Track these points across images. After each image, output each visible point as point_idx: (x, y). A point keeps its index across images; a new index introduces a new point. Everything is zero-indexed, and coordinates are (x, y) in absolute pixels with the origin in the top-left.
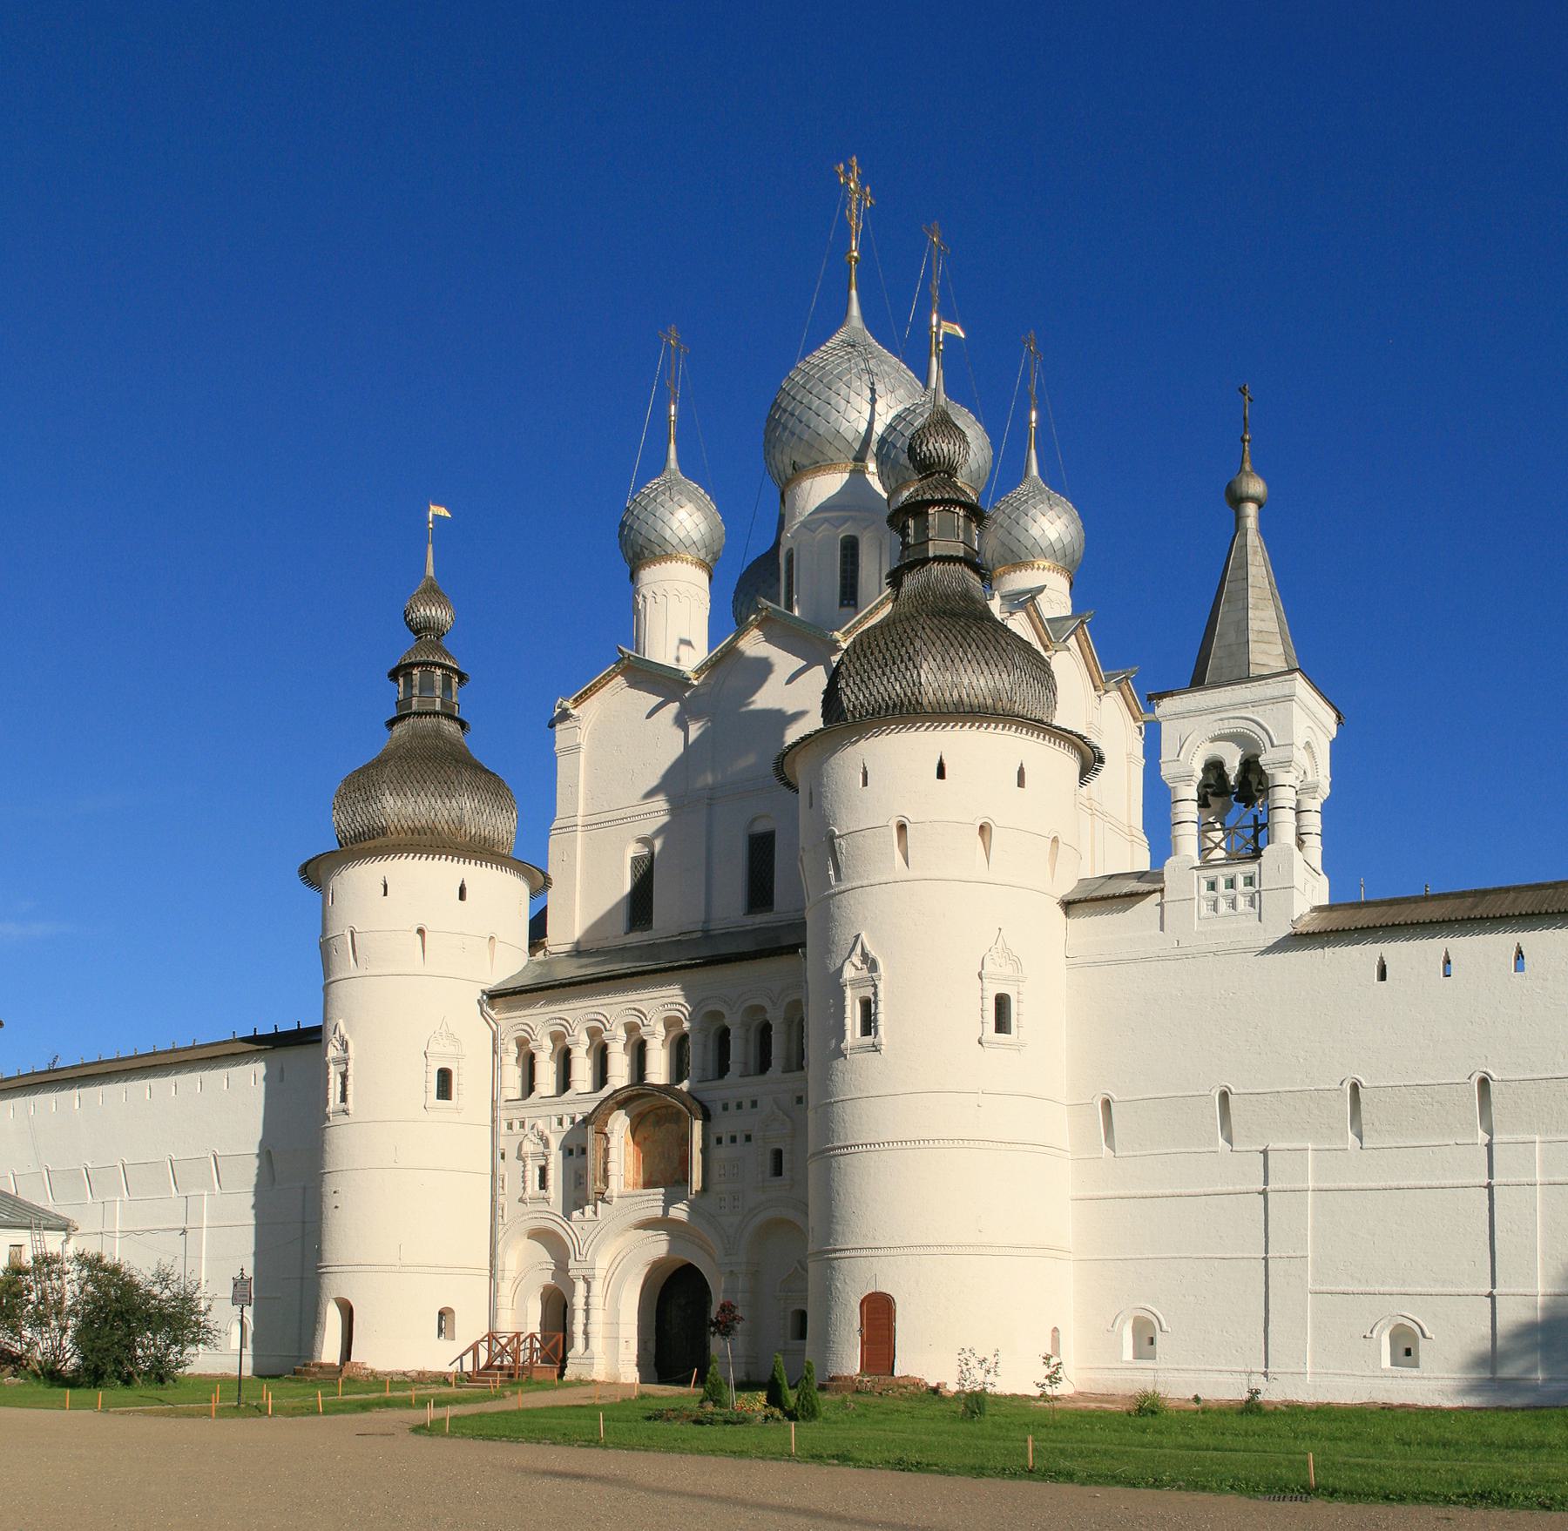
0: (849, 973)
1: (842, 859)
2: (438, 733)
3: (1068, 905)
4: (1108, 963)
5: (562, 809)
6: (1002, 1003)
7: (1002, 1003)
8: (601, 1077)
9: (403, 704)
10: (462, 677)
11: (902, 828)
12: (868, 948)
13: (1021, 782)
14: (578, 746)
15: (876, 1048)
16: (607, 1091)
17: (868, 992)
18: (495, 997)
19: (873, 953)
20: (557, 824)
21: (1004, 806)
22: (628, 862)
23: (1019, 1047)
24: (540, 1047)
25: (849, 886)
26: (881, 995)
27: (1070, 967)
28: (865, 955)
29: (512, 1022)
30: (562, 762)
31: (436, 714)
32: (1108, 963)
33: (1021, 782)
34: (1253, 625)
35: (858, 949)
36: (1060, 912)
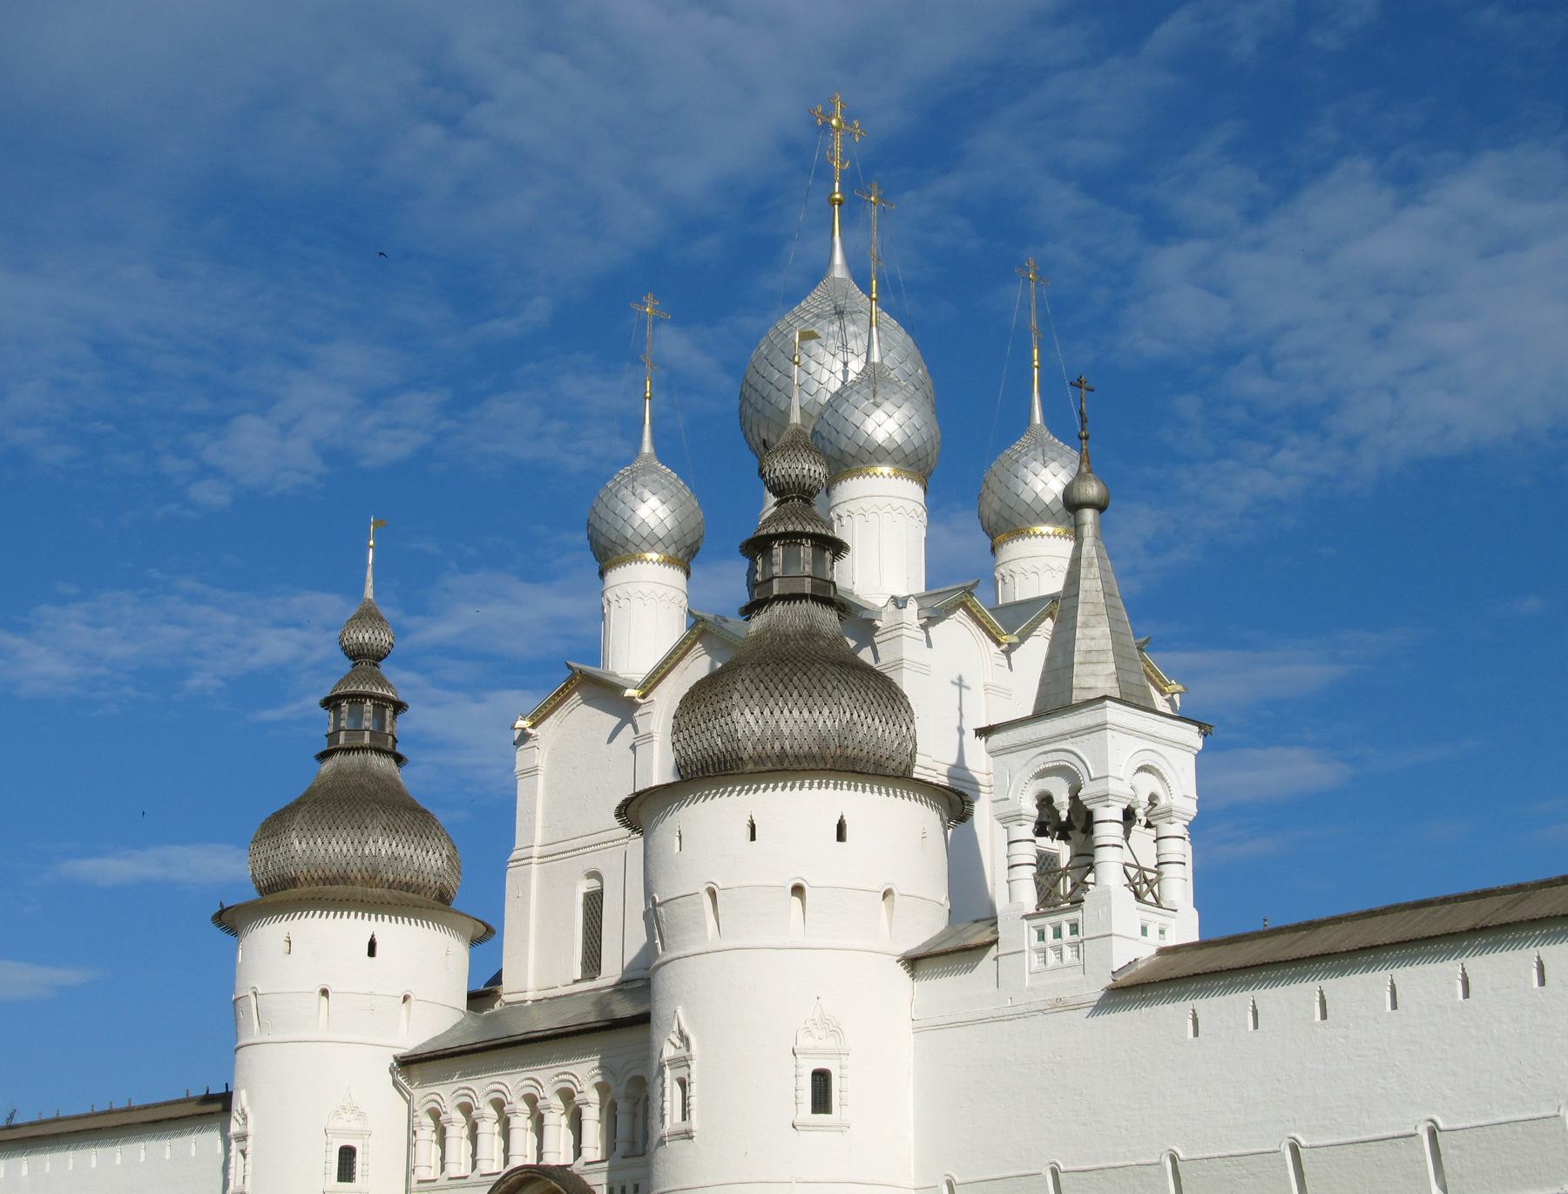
0: (669, 1052)
1: (663, 927)
2: (364, 770)
3: (914, 963)
4: (950, 1025)
5: (520, 840)
6: (821, 1079)
7: (821, 1079)
8: (506, 1162)
9: (332, 737)
10: (399, 707)
11: (713, 894)
12: (683, 1025)
13: (841, 836)
14: (535, 769)
15: (687, 1135)
16: (509, 1168)
17: (682, 1073)
18: (409, 1064)
19: (687, 1031)
20: (515, 854)
21: (820, 862)
22: (580, 900)
23: (842, 1128)
24: (450, 1122)
25: (674, 955)
26: (693, 1077)
27: (917, 1030)
28: (681, 1032)
29: (422, 1094)
30: (522, 786)
31: (364, 749)
32: (950, 1025)
33: (841, 836)
34: (1081, 645)
35: (675, 1028)
36: (901, 973)
